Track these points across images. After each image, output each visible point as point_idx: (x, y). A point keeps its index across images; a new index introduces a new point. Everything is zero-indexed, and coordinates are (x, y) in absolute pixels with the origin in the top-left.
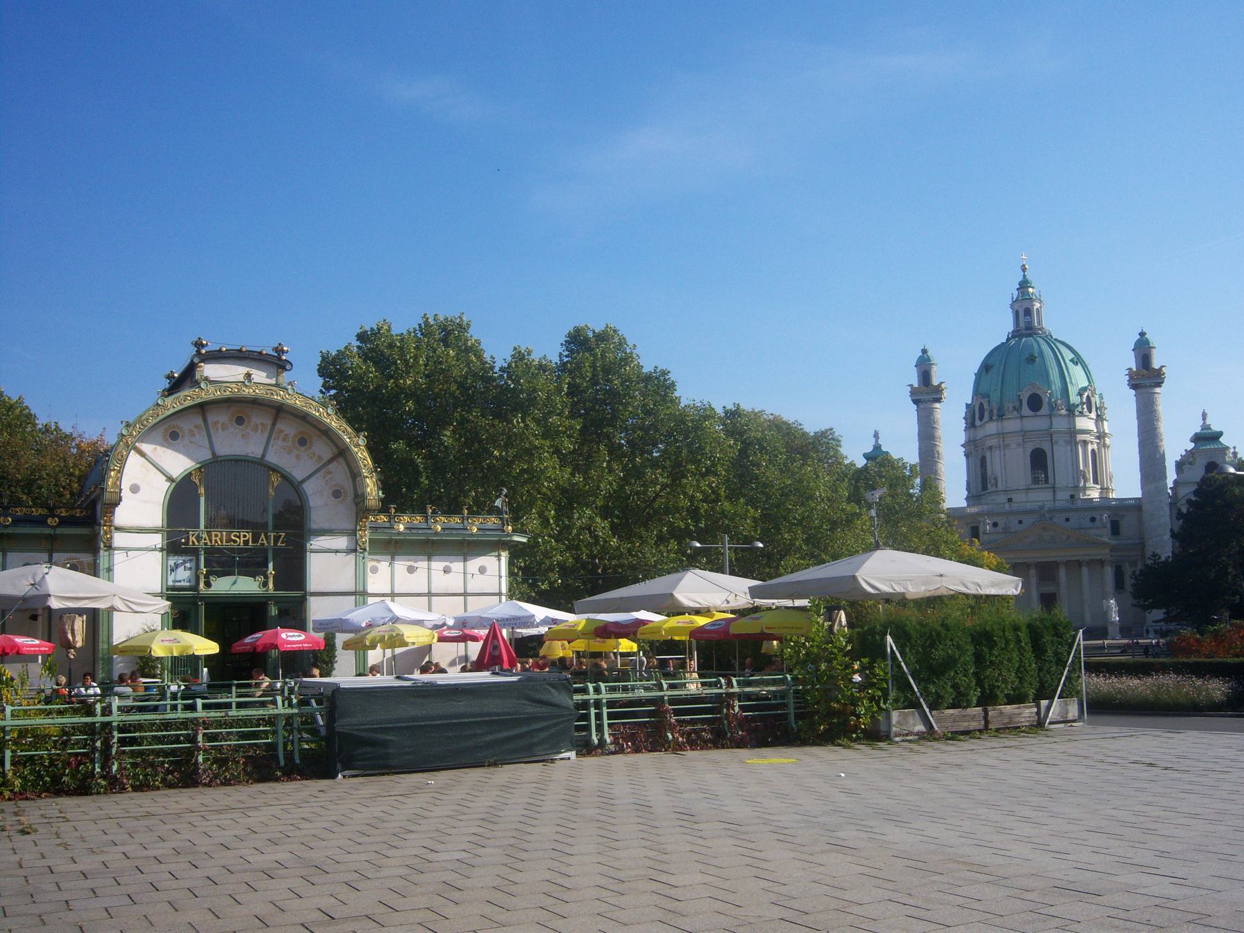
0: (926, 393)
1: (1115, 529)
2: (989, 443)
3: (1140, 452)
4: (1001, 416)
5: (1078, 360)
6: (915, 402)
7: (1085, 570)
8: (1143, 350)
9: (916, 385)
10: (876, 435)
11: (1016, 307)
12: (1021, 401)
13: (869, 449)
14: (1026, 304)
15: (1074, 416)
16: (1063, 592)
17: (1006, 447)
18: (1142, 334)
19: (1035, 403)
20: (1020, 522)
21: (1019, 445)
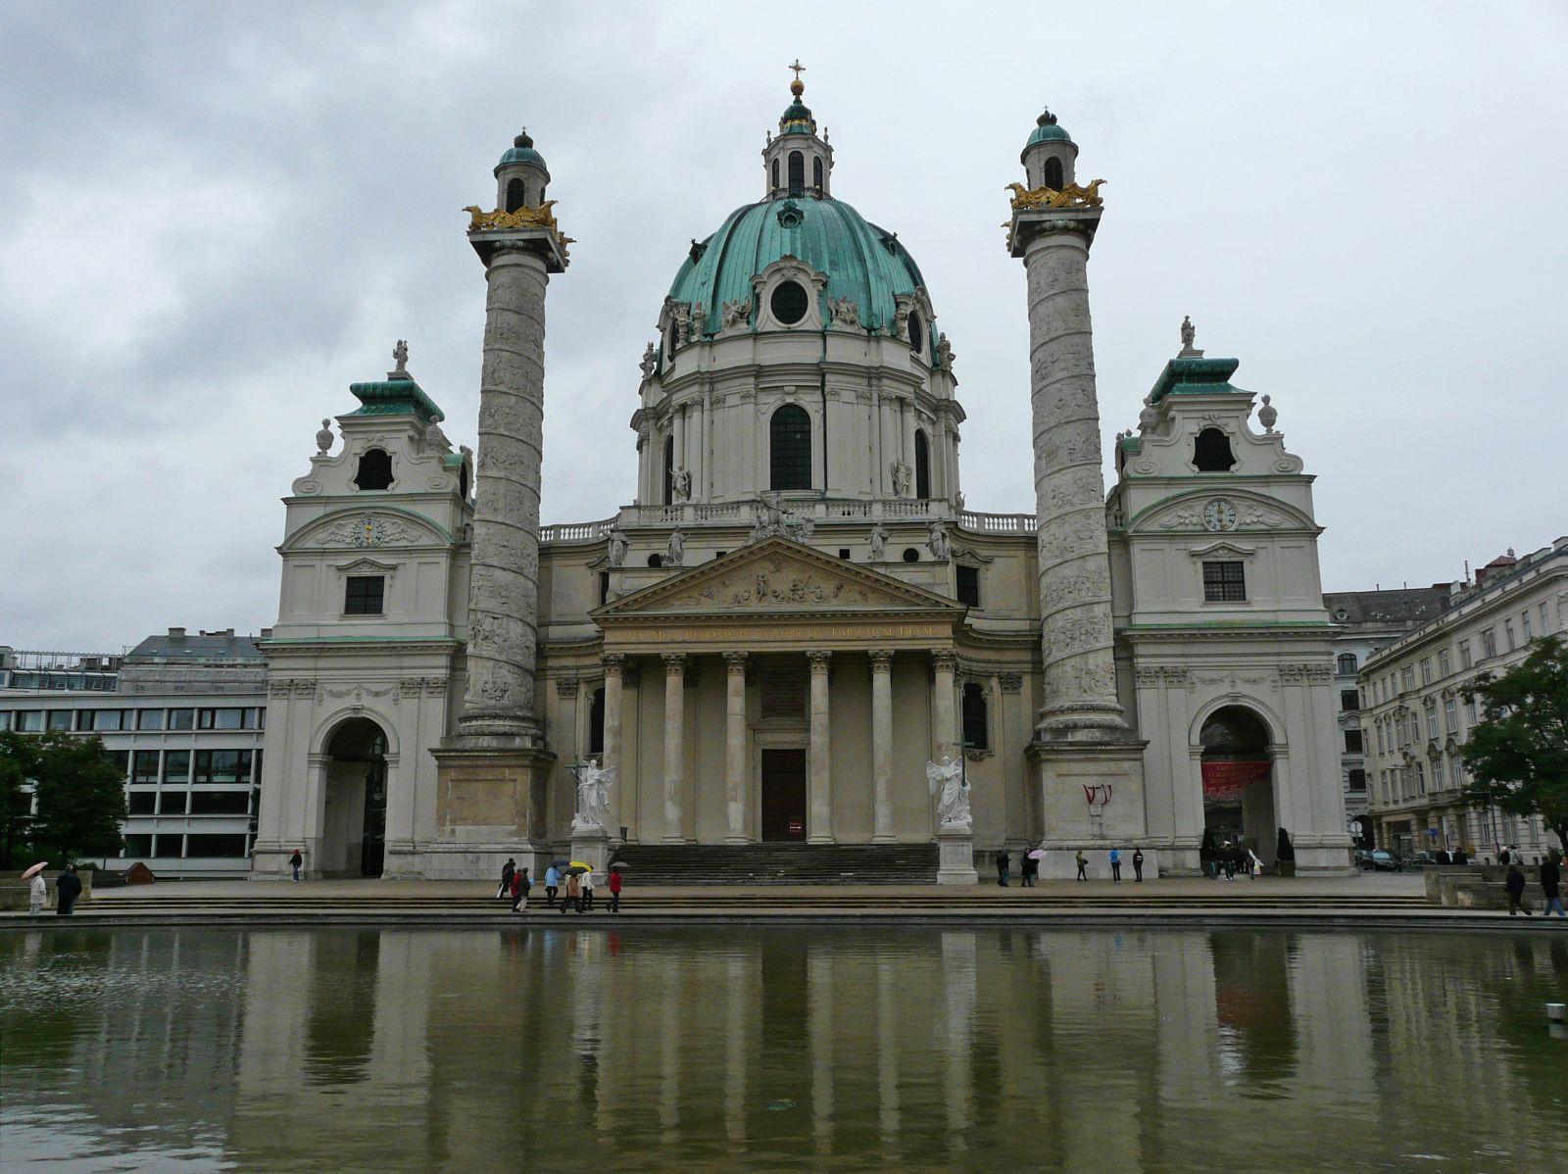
0: (520, 235)
1: (968, 585)
2: (679, 398)
3: (1037, 394)
4: (710, 340)
5: (890, 243)
6: (486, 251)
7: (882, 681)
8: (1051, 151)
10: (401, 353)
12: (757, 298)
14: (794, 145)
15: (878, 339)
16: (818, 741)
17: (718, 402)
19: (790, 303)
20: (720, 555)
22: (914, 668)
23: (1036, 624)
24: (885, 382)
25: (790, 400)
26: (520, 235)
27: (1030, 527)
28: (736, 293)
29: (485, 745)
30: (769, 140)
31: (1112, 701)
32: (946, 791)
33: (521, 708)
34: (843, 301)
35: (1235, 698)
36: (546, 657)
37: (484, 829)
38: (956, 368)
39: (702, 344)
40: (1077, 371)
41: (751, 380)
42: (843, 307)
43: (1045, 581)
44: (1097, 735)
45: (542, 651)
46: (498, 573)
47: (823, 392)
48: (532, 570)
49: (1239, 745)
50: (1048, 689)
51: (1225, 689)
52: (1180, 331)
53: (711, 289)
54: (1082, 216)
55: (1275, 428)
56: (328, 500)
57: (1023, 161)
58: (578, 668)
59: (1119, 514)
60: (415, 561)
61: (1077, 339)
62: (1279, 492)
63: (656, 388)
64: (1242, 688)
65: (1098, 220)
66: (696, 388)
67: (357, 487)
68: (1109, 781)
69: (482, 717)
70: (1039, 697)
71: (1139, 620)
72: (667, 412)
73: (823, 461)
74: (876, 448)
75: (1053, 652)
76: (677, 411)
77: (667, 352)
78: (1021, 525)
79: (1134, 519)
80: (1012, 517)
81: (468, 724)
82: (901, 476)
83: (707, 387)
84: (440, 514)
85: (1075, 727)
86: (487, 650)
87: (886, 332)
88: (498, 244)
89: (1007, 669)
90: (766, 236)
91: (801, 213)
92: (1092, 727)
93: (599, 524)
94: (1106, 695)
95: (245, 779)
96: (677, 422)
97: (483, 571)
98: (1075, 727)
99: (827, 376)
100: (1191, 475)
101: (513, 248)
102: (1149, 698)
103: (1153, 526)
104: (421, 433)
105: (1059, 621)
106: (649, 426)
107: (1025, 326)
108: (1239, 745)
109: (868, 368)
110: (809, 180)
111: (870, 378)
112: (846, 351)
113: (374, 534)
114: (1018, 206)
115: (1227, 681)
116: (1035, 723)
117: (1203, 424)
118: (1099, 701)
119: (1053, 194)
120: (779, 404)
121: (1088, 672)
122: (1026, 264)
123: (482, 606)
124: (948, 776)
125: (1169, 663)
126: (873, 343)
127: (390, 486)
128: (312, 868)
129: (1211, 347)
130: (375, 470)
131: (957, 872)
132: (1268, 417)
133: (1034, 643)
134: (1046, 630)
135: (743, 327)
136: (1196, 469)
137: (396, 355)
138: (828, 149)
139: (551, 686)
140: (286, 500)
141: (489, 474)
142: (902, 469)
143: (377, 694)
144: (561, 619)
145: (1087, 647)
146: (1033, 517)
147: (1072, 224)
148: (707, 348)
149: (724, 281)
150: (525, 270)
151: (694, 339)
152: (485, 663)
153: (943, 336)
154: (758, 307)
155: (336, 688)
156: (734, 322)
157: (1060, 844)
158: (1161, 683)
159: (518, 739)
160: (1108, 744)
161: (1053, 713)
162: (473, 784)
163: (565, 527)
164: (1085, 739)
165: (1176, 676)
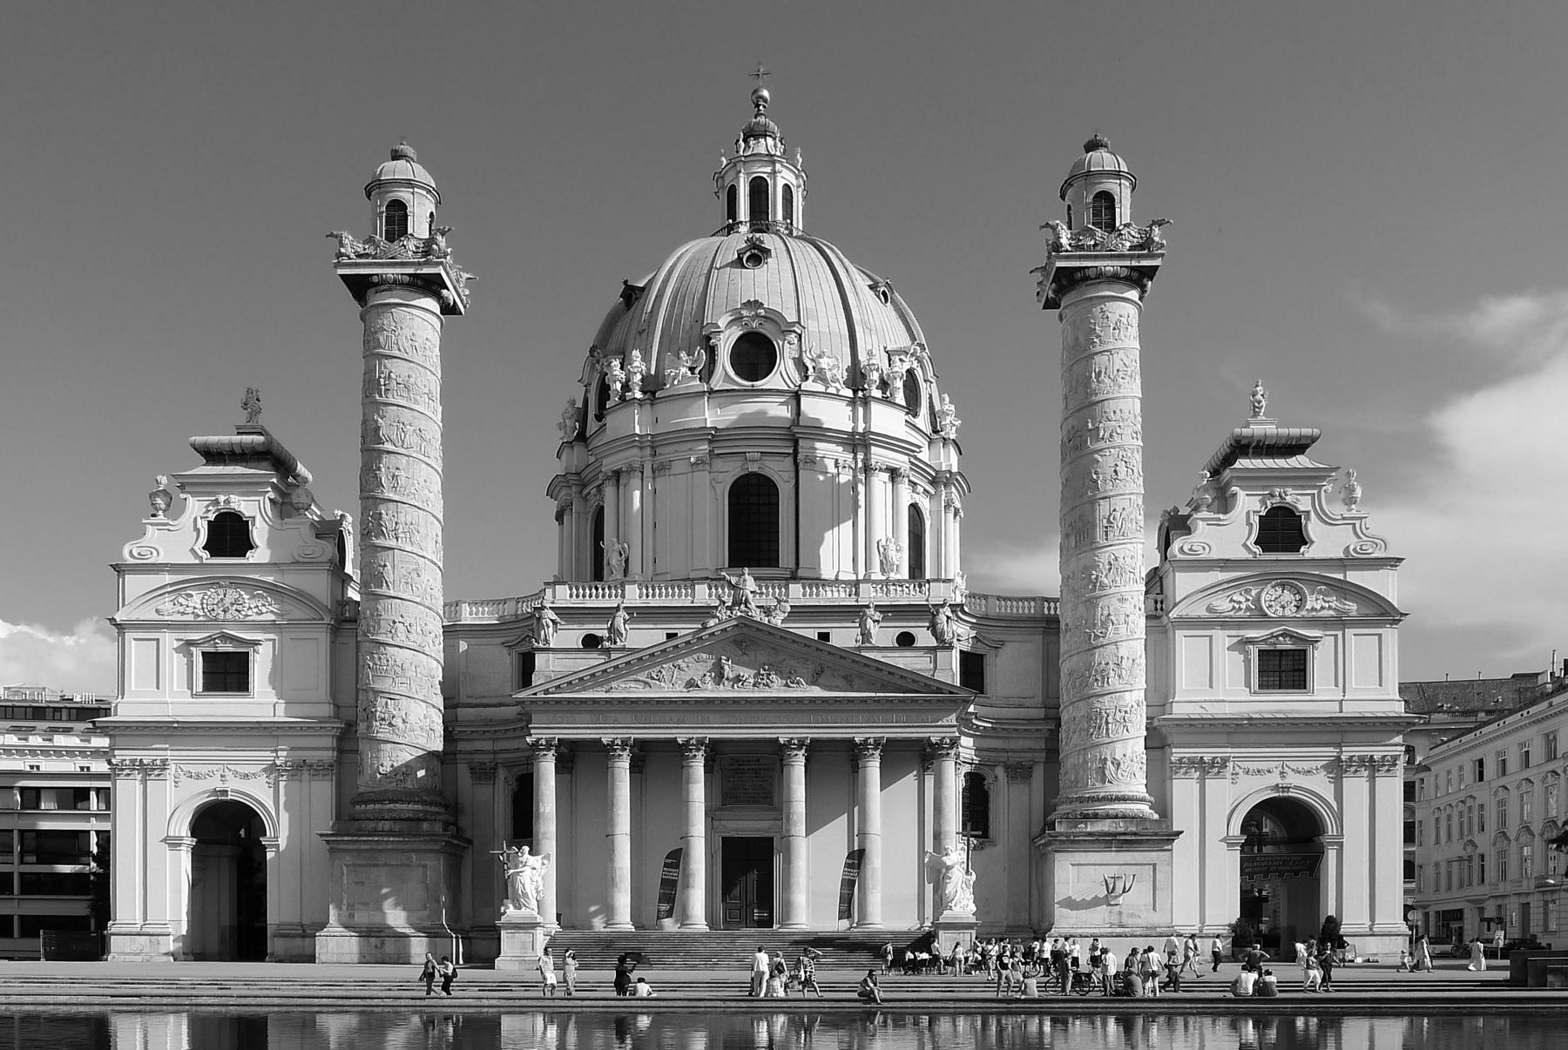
11: (728, 182)
12: (712, 352)
15: (866, 401)
19: (756, 355)
36: (456, 740)
41: (705, 447)
44: (1121, 826)
47: (795, 459)
49: (1285, 843)
59: (1159, 598)
69: (381, 802)
71: (1179, 710)
72: (595, 478)
80: (1034, 599)
85: (1096, 816)
87: (877, 393)
92: (1116, 817)
93: (518, 601)
94: (1138, 786)
98: (1096, 816)
99: (801, 442)
104: (282, 494)
108: (1285, 843)
109: (853, 433)
116: (1046, 815)
118: (1125, 790)
134: (1065, 717)
143: (246, 776)
155: (194, 769)
159: (425, 825)
160: (1135, 834)
164: (1106, 829)
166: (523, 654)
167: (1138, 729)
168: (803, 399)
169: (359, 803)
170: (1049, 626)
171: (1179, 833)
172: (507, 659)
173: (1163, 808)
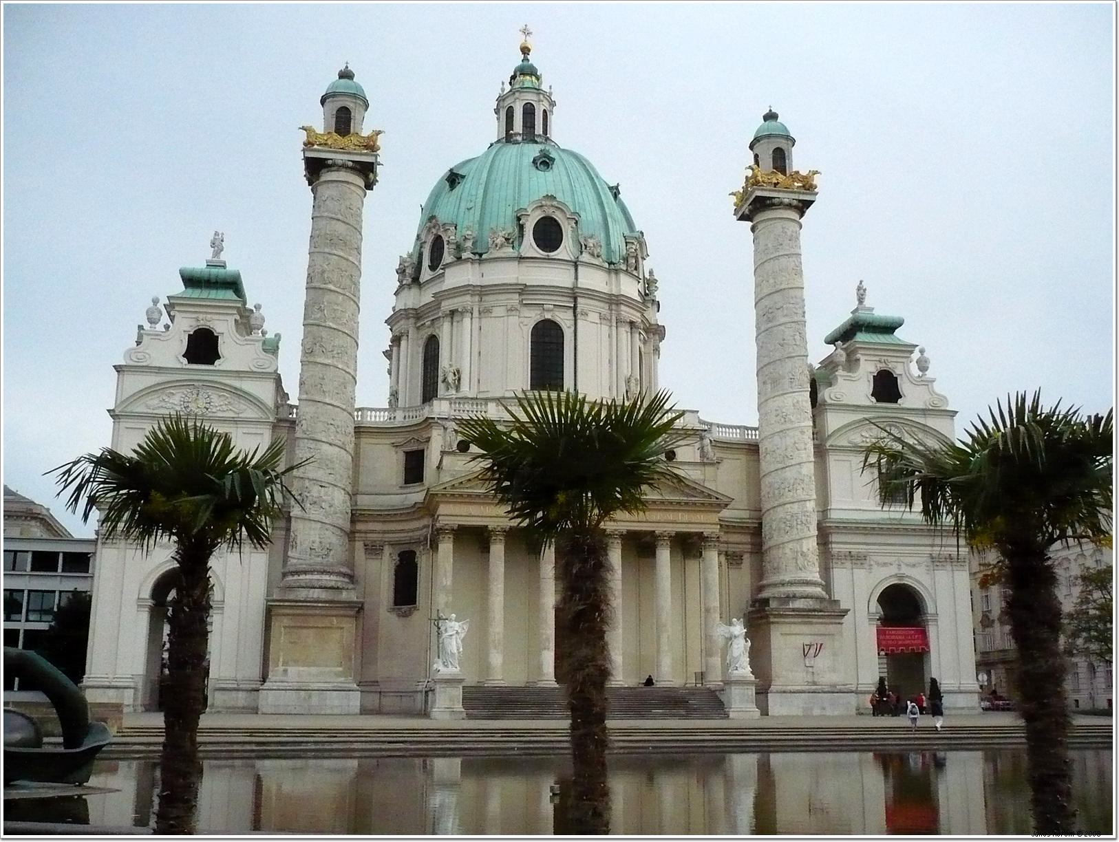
0: (340, 157)
2: (447, 305)
4: (479, 258)
5: (615, 192)
6: (315, 168)
7: (664, 555)
9: (319, 128)
10: (217, 245)
11: (508, 102)
12: (521, 227)
13: (198, 264)
14: (530, 97)
15: (617, 271)
18: (771, 117)
19: (549, 235)
21: (511, 310)
22: (688, 546)
23: (755, 514)
24: (623, 307)
25: (548, 316)
26: (340, 157)
27: (752, 436)
28: (502, 220)
29: (315, 596)
30: (503, 90)
31: (816, 577)
32: (735, 646)
33: (342, 565)
34: (591, 237)
35: (901, 577)
37: (314, 670)
38: (658, 296)
39: (473, 261)
40: (796, 319)
42: (591, 243)
43: (766, 482)
44: (810, 604)
45: (356, 516)
46: (325, 447)
48: (350, 448)
50: (768, 566)
51: (893, 570)
52: (855, 292)
53: (478, 214)
54: (802, 197)
55: (929, 374)
56: (160, 370)
57: (751, 147)
58: (384, 532)
60: (240, 430)
61: (797, 292)
62: (932, 422)
63: (415, 290)
64: (905, 570)
65: (812, 202)
66: (468, 298)
67: (185, 361)
68: (819, 640)
69: (312, 572)
70: (759, 572)
71: (834, 515)
73: (579, 370)
74: (615, 362)
75: (773, 535)
76: (447, 316)
77: (426, 262)
78: (742, 434)
79: (830, 436)
80: (739, 427)
81: (296, 577)
82: (632, 384)
83: (477, 298)
84: (265, 392)
85: (795, 597)
86: (313, 513)
88: (330, 162)
89: (732, 549)
90: (525, 176)
91: (553, 160)
94: (814, 574)
95: (14, 617)
96: (446, 326)
97: (312, 445)
98: (795, 597)
99: (579, 300)
100: (868, 403)
101: (344, 167)
102: (840, 575)
103: (843, 442)
105: (781, 513)
106: (406, 325)
107: (752, 280)
110: (539, 129)
111: (610, 304)
112: (593, 279)
113: (201, 403)
114: (753, 182)
115: (895, 566)
117: (879, 365)
119: (780, 176)
120: (539, 318)
121: (803, 554)
122: (753, 229)
123: (311, 476)
124: (736, 633)
125: (855, 549)
126: (613, 275)
127: (217, 362)
128: (139, 702)
129: (881, 311)
130: (203, 347)
131: (742, 709)
132: (923, 366)
133: (756, 531)
135: (509, 251)
136: (874, 399)
137: (213, 245)
138: (553, 104)
139: (359, 545)
140: (119, 369)
141: (319, 360)
142: (633, 380)
144: (369, 490)
145: (802, 535)
146: (755, 429)
147: (795, 203)
148: (477, 265)
149: (488, 210)
150: (353, 188)
151: (465, 255)
152: (314, 525)
153: (651, 273)
154: (521, 235)
156: (502, 246)
157: (785, 688)
158: (848, 564)
161: (775, 585)
162: (304, 631)
163: (372, 410)
165: (858, 560)
166: (407, 453)
167: (814, 532)
168: (580, 268)
169: (293, 573)
170: (753, 449)
171: (847, 611)
172: (395, 457)
173: (828, 587)
